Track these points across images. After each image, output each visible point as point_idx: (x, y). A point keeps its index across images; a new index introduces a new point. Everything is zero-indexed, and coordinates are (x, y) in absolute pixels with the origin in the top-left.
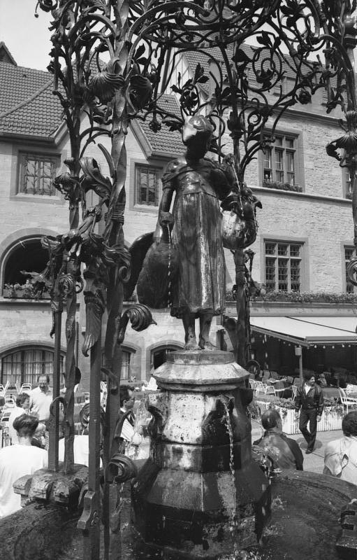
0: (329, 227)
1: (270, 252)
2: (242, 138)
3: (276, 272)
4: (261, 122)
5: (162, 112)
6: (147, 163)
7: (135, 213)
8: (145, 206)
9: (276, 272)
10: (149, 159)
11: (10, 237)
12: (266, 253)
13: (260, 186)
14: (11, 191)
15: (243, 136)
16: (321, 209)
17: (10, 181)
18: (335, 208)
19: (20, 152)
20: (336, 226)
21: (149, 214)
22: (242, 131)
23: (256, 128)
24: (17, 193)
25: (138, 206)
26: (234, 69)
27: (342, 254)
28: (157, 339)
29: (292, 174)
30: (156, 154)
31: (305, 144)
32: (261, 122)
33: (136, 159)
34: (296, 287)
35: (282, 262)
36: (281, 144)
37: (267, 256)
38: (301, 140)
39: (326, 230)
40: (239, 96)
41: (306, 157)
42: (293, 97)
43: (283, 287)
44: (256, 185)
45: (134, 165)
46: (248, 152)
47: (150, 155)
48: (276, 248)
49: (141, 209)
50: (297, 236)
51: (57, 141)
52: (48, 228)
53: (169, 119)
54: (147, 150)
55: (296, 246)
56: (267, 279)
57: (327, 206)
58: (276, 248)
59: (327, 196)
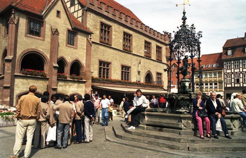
0: (118, 59)
6: (72, 30)
7: (67, 47)
10: (72, 29)
11: (24, 51)
14: (25, 33)
17: (25, 29)
18: (116, 52)
19: (29, 18)
27: (121, 68)
28: (72, 92)
29: (108, 40)
31: (113, 30)
34: (107, 77)
36: (106, 29)
39: (117, 60)
41: (113, 34)
43: (104, 77)
47: (73, 27)
48: (102, 64)
50: (109, 61)
52: (39, 49)
54: (73, 26)
57: (118, 52)
59: (118, 48)
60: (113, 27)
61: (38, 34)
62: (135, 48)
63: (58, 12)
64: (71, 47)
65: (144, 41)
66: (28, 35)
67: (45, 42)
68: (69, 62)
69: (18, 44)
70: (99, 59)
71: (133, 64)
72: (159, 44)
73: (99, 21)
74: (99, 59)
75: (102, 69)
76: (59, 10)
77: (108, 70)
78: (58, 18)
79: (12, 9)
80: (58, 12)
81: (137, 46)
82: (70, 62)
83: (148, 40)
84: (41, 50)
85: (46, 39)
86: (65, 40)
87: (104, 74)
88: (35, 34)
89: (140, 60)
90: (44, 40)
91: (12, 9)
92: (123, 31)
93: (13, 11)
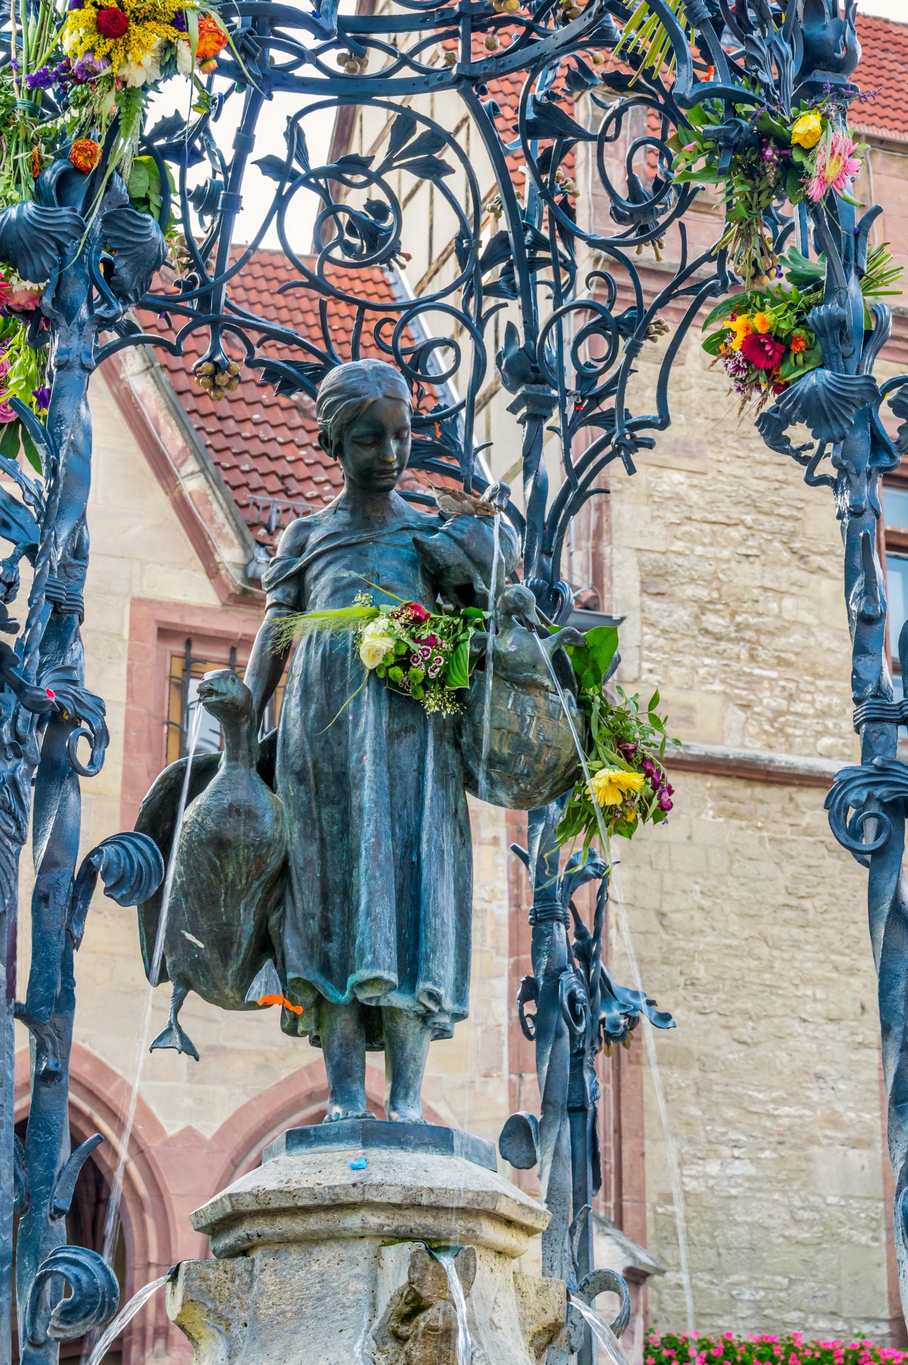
2: (555, 419)
4: (621, 359)
5: (240, 328)
15: (556, 412)
22: (555, 393)
23: (602, 381)
26: (523, 171)
32: (621, 359)
40: (545, 262)
42: (721, 267)
45: (152, 631)
46: (573, 473)
53: (273, 353)
68: (189, 1134)
82: (209, 1130)
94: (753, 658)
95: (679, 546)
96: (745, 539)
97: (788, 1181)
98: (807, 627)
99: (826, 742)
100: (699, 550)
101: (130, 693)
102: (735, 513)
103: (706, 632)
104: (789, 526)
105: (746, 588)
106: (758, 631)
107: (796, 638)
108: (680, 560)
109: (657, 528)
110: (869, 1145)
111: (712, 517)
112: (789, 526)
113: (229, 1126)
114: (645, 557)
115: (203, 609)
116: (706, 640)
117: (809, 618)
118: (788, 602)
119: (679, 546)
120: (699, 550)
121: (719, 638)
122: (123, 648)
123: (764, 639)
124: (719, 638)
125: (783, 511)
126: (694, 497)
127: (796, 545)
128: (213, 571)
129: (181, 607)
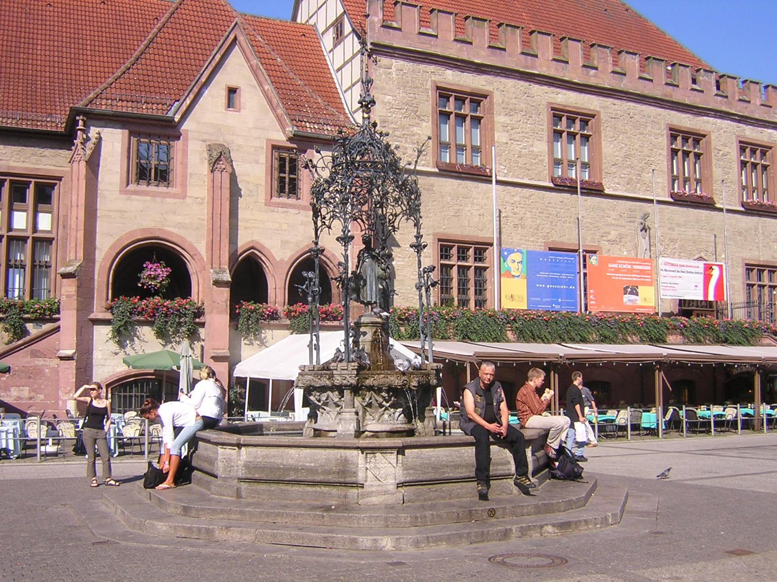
1: (447, 257)
3: (455, 284)
7: (272, 208)
8: (284, 200)
9: (455, 284)
12: (442, 258)
13: (434, 167)
14: (121, 182)
16: (517, 199)
20: (538, 221)
21: (290, 210)
24: (128, 184)
25: (275, 199)
30: (299, 133)
33: (272, 140)
34: (480, 303)
35: (463, 270)
37: (443, 262)
38: (491, 103)
41: (497, 126)
43: (464, 303)
44: (428, 166)
48: (454, 251)
49: (279, 204)
51: (176, 120)
52: (166, 228)
55: (481, 249)
56: (442, 293)
58: (454, 251)
60: (497, 98)
61: (163, 176)
62: (614, 169)
63: (232, 91)
64: (284, 206)
65: (665, 133)
66: (132, 187)
67: (188, 200)
68: (282, 260)
69: (98, 219)
70: (434, 235)
71: (611, 237)
72: (751, 133)
73: (429, 85)
74: (434, 235)
75: (455, 269)
76: (233, 84)
77: (480, 271)
78: (231, 113)
79: (77, 118)
80: (232, 91)
81: (627, 156)
82: (286, 260)
83: (686, 121)
84: (175, 231)
85: (192, 191)
86: (264, 183)
87: (463, 290)
88: (156, 179)
89: (645, 217)
90: (184, 196)
91: (77, 118)
92: (549, 103)
93: (81, 123)
94: (406, 141)
95: (390, 114)
96: (406, 112)
97: (411, 265)
98: (419, 134)
99: (423, 162)
100: (394, 115)
101: (266, 161)
102: (403, 106)
103: (395, 136)
104: (416, 109)
105: (405, 125)
106: (407, 135)
107: (416, 137)
108: (390, 118)
109: (384, 110)
110: (430, 257)
111: (398, 107)
112: (416, 109)
113: (290, 258)
114: (381, 118)
115: (282, 141)
116: (396, 138)
117: (420, 133)
118: (415, 128)
119: (390, 114)
120: (394, 115)
121: (399, 137)
122: (265, 151)
123: (408, 137)
124: (399, 137)
125: (414, 105)
126: (393, 102)
127: (417, 114)
128: (284, 133)
129: (277, 141)
